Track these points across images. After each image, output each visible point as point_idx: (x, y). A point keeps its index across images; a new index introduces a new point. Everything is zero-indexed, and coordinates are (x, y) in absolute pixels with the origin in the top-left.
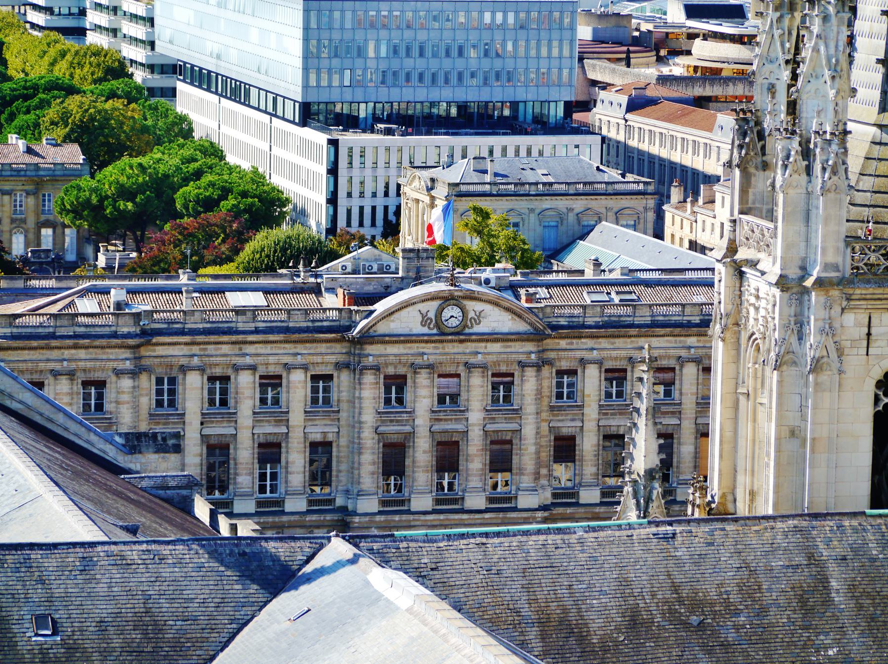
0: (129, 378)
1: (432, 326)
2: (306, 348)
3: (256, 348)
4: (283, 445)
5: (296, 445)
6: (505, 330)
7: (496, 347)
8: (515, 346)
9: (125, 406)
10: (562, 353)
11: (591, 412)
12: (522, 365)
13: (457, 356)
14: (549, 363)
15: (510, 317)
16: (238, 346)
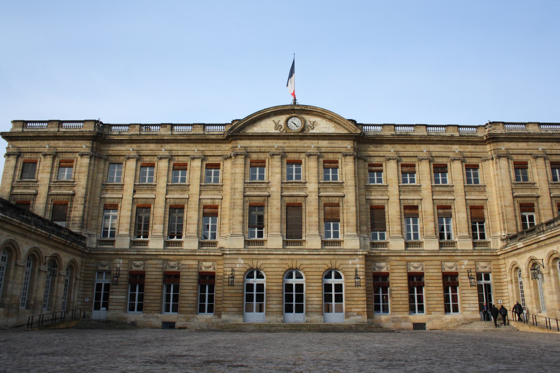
0: (87, 158)
1: (282, 130)
2: (202, 147)
3: (171, 146)
4: (186, 206)
5: (193, 206)
7: (324, 144)
8: (337, 143)
9: (83, 174)
13: (298, 148)
15: (333, 125)
16: (160, 145)
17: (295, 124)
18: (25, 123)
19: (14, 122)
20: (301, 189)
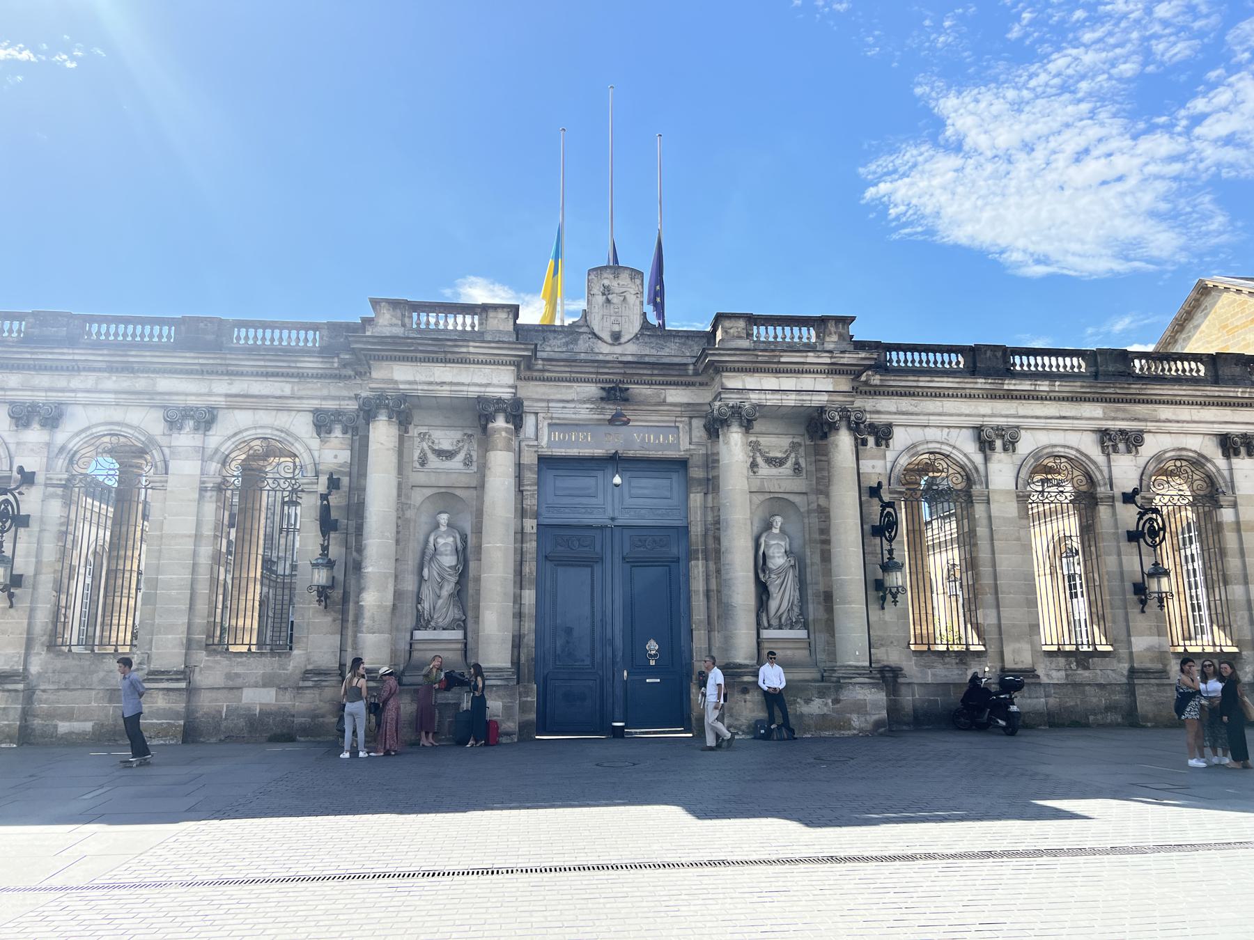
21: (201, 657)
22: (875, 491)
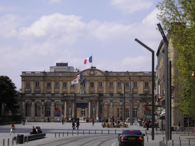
6: (101, 75)
7: (99, 78)
10: (110, 79)
11: (115, 89)
12: (104, 80)
14: (109, 81)
17: (92, 73)
18: (25, 72)
19: (22, 72)
20: (94, 89)
21: (54, 117)
22: (101, 105)
